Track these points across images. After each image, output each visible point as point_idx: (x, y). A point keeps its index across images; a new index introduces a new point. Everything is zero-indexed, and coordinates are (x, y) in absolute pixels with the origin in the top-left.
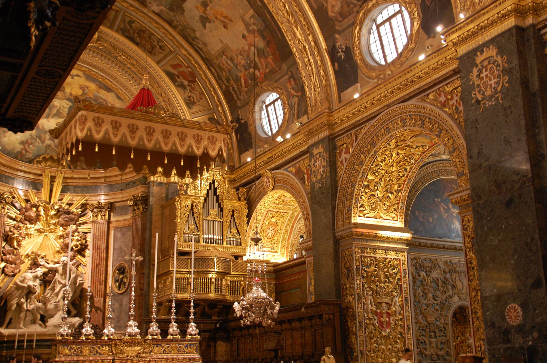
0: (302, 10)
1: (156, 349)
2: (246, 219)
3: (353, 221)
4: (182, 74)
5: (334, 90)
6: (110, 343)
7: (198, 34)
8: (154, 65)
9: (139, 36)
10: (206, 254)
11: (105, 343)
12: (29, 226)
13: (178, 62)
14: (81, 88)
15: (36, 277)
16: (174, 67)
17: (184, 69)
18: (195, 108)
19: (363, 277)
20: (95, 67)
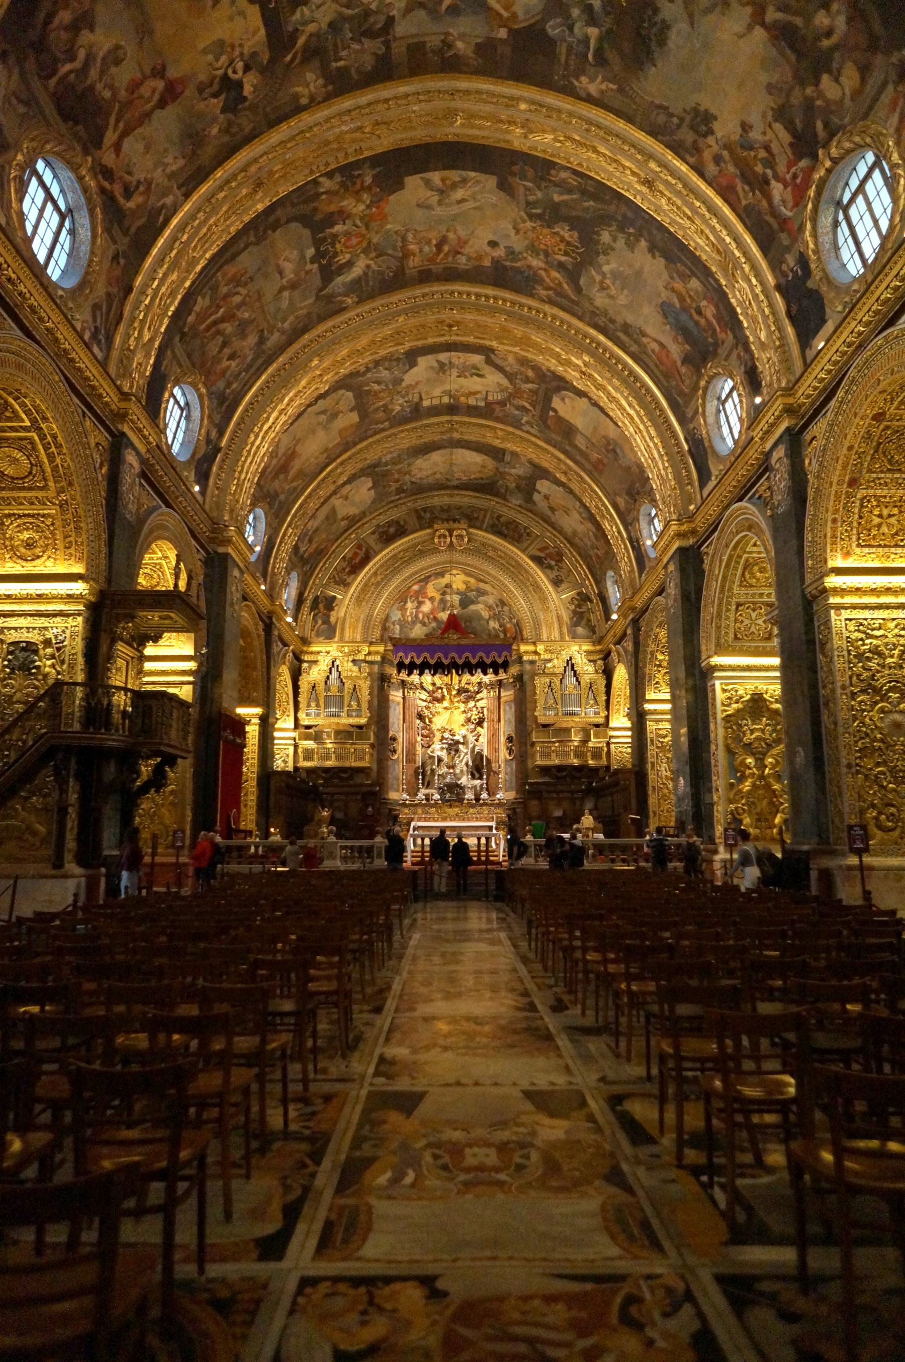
0: (604, 504)
1: (471, 810)
2: (604, 690)
3: (647, 697)
4: (550, 556)
5: (637, 574)
6: (436, 805)
7: (553, 519)
8: (519, 553)
9: (507, 528)
10: (564, 725)
11: (432, 806)
12: (437, 705)
13: (544, 545)
14: (465, 583)
15: (442, 748)
16: (541, 550)
17: (551, 550)
18: (563, 586)
19: (658, 747)
20: (469, 565)
